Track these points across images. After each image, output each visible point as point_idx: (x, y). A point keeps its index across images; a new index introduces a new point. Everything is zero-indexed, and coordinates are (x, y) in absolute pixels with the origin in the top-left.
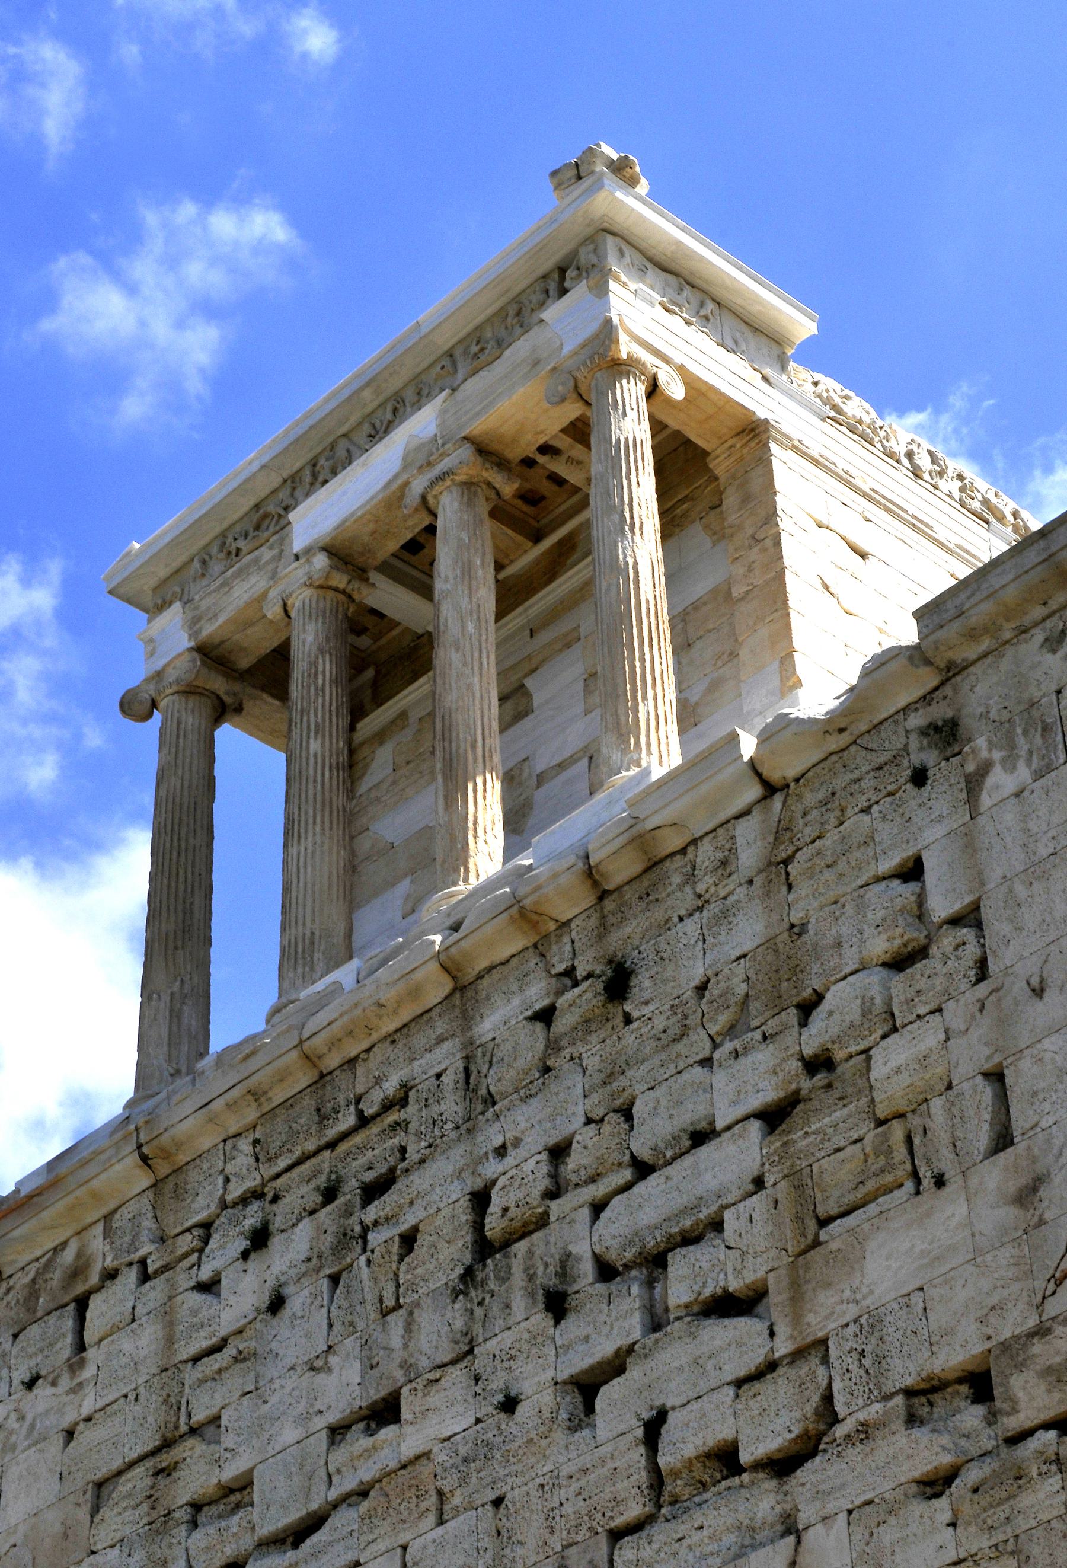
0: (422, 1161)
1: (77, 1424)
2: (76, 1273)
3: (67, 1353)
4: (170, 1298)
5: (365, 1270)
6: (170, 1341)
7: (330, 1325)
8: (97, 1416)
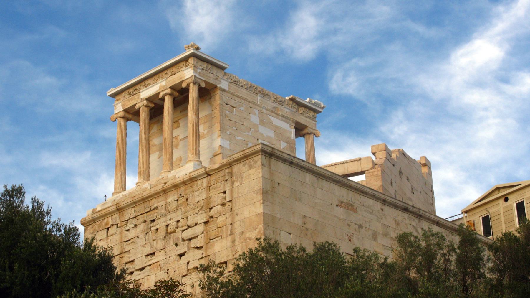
0: (159, 219)
5: (151, 233)
6: (122, 238)
7: (146, 241)
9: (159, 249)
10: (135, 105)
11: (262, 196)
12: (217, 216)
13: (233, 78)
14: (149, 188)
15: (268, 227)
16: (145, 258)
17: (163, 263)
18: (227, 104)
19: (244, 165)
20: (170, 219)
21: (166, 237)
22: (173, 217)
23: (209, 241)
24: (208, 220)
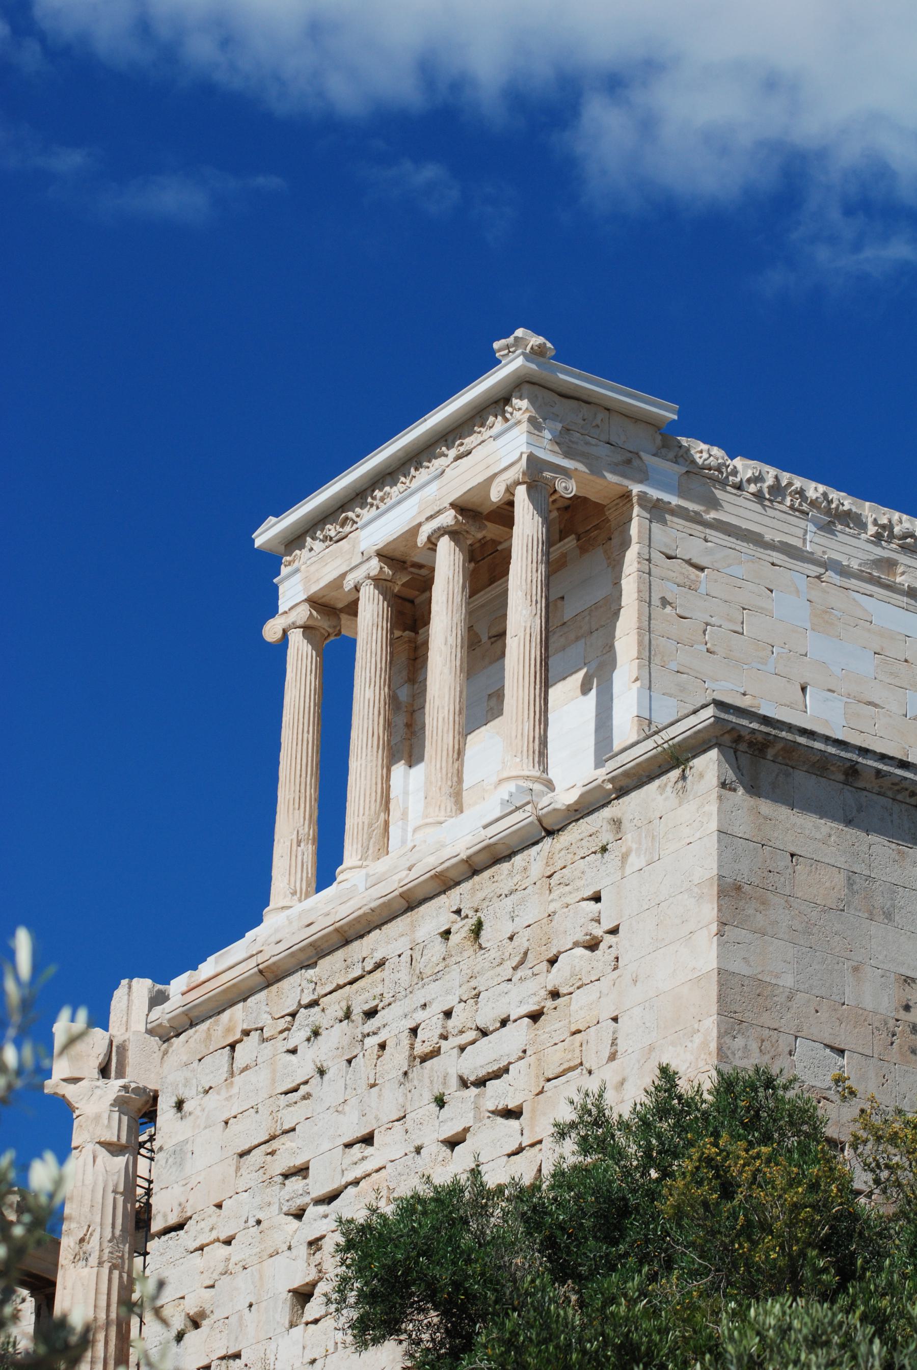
0: (390, 1004)
1: (229, 1119)
2: (229, 1030)
3: (225, 1076)
4: (274, 1056)
6: (273, 1081)
7: (346, 1088)
8: (238, 1116)
9: (386, 1120)
10: (343, 576)
11: (715, 906)
12: (571, 989)
13: (698, 455)
14: (361, 888)
15: (737, 1027)
16: (344, 1153)
17: (396, 1173)
18: (669, 557)
19: (662, 789)
20: (425, 1005)
21: (410, 1071)
22: (434, 996)
23: (542, 1083)
24: (542, 1004)
